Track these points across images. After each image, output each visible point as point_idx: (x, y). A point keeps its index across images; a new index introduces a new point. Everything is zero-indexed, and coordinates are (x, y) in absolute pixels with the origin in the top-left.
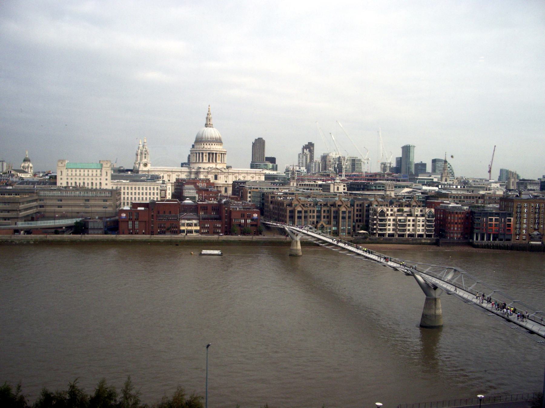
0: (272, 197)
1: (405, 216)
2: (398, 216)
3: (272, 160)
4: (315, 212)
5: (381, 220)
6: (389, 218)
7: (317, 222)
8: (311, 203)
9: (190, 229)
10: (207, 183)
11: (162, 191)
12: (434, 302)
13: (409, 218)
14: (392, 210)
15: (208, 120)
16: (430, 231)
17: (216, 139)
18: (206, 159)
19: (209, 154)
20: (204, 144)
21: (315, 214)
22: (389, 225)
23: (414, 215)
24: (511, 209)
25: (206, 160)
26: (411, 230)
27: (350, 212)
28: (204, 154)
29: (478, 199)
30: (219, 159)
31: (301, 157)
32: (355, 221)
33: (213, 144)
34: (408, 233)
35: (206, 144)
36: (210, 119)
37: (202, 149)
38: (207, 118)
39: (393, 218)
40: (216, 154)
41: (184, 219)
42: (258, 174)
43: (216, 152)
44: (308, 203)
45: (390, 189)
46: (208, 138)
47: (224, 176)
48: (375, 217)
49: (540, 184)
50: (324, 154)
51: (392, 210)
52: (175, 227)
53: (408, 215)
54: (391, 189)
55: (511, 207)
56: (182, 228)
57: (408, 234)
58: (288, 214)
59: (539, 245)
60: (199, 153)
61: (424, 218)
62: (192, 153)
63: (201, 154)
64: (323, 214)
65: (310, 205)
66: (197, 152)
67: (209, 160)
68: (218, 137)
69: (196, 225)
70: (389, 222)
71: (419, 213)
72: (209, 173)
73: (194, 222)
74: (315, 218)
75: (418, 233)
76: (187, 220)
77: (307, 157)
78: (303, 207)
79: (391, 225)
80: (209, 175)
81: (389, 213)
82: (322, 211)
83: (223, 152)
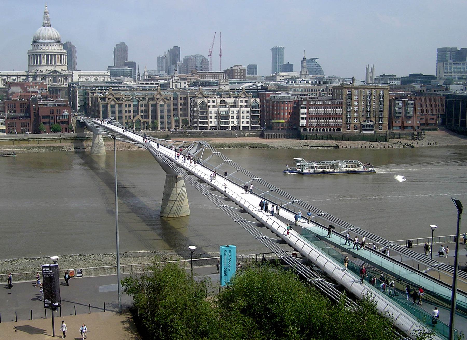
0: (91, 93)
1: (228, 108)
2: (221, 108)
3: (132, 65)
4: (132, 106)
5: (202, 112)
6: (210, 109)
7: (134, 117)
8: (128, 96)
12: (175, 180)
13: (232, 109)
14: (214, 102)
15: (46, 19)
16: (256, 122)
17: (54, 39)
18: (44, 61)
20: (41, 45)
21: (132, 109)
22: (211, 118)
23: (238, 106)
24: (341, 96)
25: (44, 62)
26: (235, 123)
27: (169, 105)
29: (321, 91)
31: (160, 60)
32: (179, 116)
34: (232, 125)
35: (44, 45)
36: (47, 18)
38: (44, 17)
39: (216, 109)
42: (101, 76)
44: (125, 96)
45: (224, 83)
46: (45, 39)
47: (64, 79)
48: (195, 109)
49: (400, 80)
50: (186, 57)
51: (214, 102)
53: (231, 107)
54: (225, 83)
55: (341, 95)
57: (231, 127)
58: (101, 109)
59: (371, 134)
60: (37, 55)
61: (249, 109)
62: (29, 55)
64: (140, 109)
65: (123, 99)
67: (47, 63)
68: (52, 37)
70: (210, 115)
71: (244, 104)
72: (47, 76)
74: (132, 112)
75: (242, 125)
77: (167, 60)
79: (213, 117)
81: (211, 104)
82: (139, 104)
83: (63, 54)
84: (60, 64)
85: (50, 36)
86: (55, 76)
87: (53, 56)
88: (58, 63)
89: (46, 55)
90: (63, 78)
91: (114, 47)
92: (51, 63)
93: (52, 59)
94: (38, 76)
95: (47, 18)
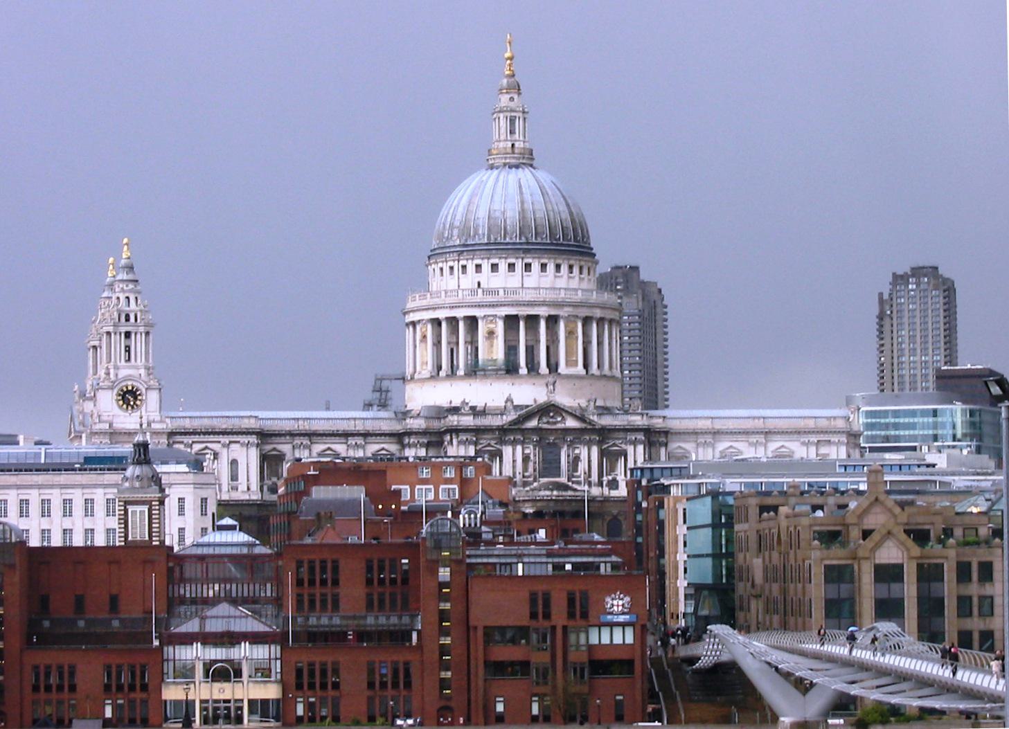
9: (227, 695)
10: (464, 482)
11: (131, 509)
19: (511, 321)
28: (482, 328)
30: (570, 352)
33: (536, 266)
35: (494, 267)
37: (469, 299)
40: (552, 321)
41: (188, 639)
42: (814, 439)
43: (553, 312)
47: (602, 454)
52: (132, 688)
56: (172, 693)
63: (461, 325)
66: (441, 314)
69: (263, 672)
73: (244, 651)
76: (204, 643)
78: (910, 542)
80: (507, 451)
83: (598, 313)
84: (584, 372)
85: (530, 215)
86: (552, 439)
87: (543, 324)
88: (571, 363)
89: (500, 324)
90: (595, 450)
91: (881, 295)
92: (532, 367)
93: (538, 341)
94: (463, 437)
95: (512, 121)
